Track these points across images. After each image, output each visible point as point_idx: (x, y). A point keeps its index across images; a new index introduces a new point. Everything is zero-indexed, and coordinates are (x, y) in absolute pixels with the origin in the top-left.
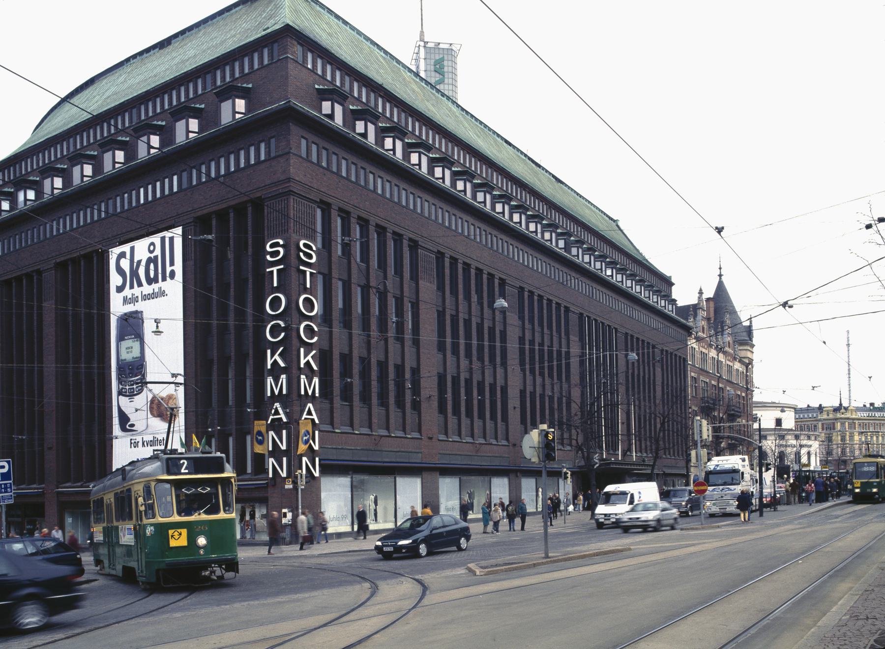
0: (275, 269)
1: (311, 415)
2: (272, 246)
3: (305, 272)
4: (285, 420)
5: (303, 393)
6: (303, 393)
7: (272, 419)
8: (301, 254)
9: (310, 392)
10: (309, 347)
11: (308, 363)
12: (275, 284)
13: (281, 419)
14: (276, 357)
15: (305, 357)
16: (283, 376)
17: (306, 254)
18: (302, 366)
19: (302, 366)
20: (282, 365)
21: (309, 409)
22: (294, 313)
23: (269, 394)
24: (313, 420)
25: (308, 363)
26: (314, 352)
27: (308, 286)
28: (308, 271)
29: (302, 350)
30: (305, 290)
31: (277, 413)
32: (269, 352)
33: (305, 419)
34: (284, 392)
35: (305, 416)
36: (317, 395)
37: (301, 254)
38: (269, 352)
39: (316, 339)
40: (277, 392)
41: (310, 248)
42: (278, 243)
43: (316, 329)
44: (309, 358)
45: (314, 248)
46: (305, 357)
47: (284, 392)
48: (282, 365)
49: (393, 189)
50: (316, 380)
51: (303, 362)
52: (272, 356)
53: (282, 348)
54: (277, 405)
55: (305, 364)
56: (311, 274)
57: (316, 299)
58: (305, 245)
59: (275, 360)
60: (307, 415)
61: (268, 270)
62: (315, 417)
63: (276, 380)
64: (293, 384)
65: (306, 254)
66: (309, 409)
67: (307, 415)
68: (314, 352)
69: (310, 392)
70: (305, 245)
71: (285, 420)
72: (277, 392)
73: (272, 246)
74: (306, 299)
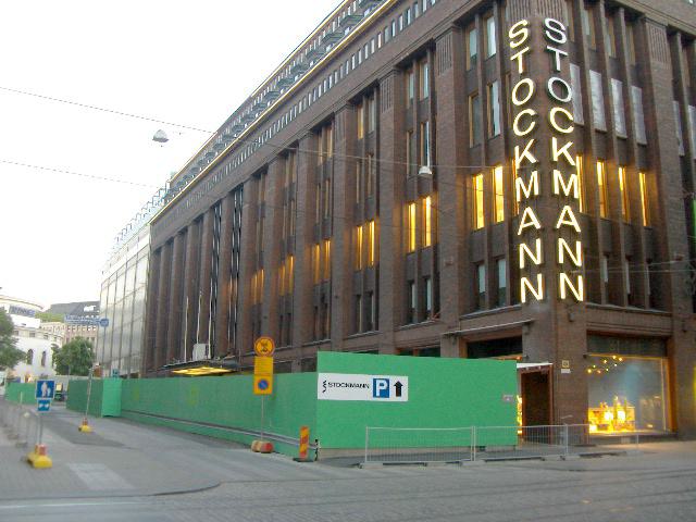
0: (519, 55)
2: (515, 31)
4: (538, 226)
8: (548, 33)
9: (567, 192)
10: (563, 138)
11: (562, 157)
12: (521, 70)
13: (533, 227)
14: (526, 153)
15: (559, 148)
16: (535, 175)
17: (552, 33)
18: (555, 159)
19: (555, 159)
20: (532, 160)
21: (567, 213)
22: (542, 98)
23: (518, 199)
24: (572, 228)
25: (562, 157)
27: (558, 68)
28: (558, 52)
29: (554, 141)
30: (556, 72)
31: (528, 219)
32: (517, 149)
33: (563, 225)
34: (536, 192)
35: (561, 221)
36: (576, 196)
37: (548, 33)
38: (517, 149)
39: (570, 130)
40: (527, 194)
41: (558, 27)
44: (564, 150)
45: (563, 28)
46: (559, 148)
47: (536, 192)
48: (532, 160)
52: (521, 151)
53: (532, 141)
54: (529, 210)
55: (559, 157)
57: (569, 83)
58: (551, 23)
61: (512, 58)
63: (526, 183)
64: (546, 181)
65: (552, 33)
66: (567, 213)
68: (569, 144)
70: (551, 23)
71: (538, 226)
72: (527, 194)
73: (515, 31)
74: (555, 83)
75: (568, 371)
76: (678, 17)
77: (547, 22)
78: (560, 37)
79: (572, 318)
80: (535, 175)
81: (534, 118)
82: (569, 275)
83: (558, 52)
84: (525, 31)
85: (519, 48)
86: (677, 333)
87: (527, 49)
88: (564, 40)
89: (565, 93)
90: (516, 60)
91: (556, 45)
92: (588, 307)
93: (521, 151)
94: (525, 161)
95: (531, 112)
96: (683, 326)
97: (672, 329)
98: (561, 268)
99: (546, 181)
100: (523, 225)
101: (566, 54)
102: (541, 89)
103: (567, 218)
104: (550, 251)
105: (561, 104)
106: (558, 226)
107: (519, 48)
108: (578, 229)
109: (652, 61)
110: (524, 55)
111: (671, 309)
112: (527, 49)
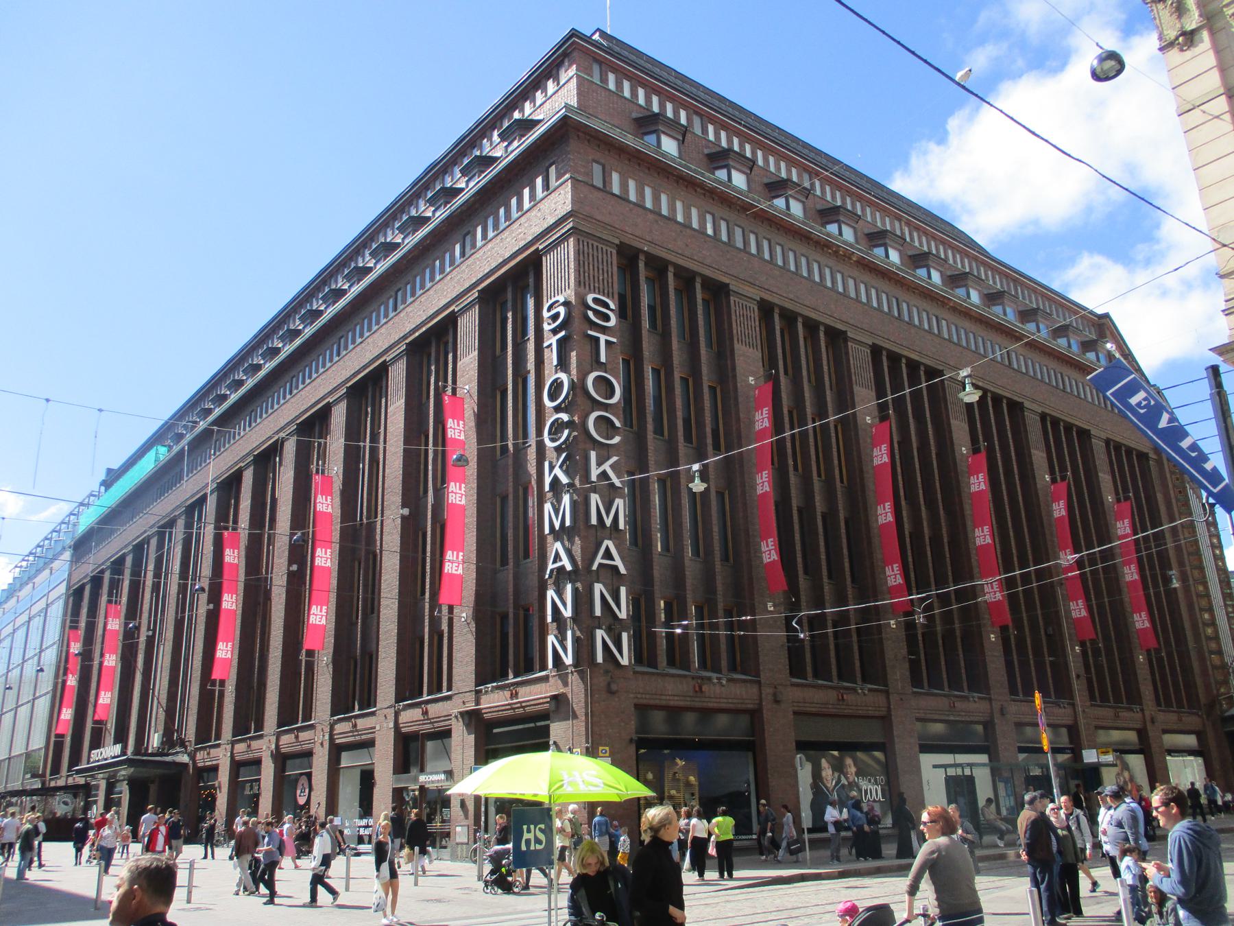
1: (612, 559)
3: (597, 339)
4: (569, 567)
5: (594, 521)
6: (594, 521)
7: (552, 571)
8: (590, 314)
9: (608, 522)
11: (604, 475)
13: (563, 567)
15: (599, 464)
16: (566, 499)
20: (564, 479)
21: (607, 549)
22: (581, 400)
24: (616, 568)
25: (604, 475)
26: (615, 459)
27: (603, 359)
28: (603, 338)
29: (593, 455)
30: (598, 365)
31: (557, 558)
33: (600, 564)
34: (568, 523)
35: (599, 560)
36: (622, 526)
37: (590, 314)
39: (617, 440)
40: (557, 525)
41: (606, 306)
42: (557, 301)
43: (618, 424)
44: (606, 467)
45: (612, 306)
46: (599, 464)
47: (568, 523)
48: (564, 479)
49: (746, 238)
50: (619, 503)
51: (594, 473)
52: (552, 468)
55: (598, 476)
56: (607, 342)
57: (617, 378)
58: (595, 300)
59: (555, 476)
60: (602, 558)
62: (618, 562)
67: (602, 558)
68: (615, 459)
69: (608, 522)
70: (595, 300)
71: (569, 567)
72: (557, 525)
73: (549, 310)
75: (678, 761)
76: (775, 290)
77: (590, 299)
78: (607, 318)
79: (614, 687)
80: (566, 499)
81: (570, 424)
82: (609, 630)
83: (603, 338)
84: (562, 310)
85: (555, 332)
86: (767, 705)
87: (563, 333)
88: (613, 322)
89: (612, 393)
90: (550, 345)
91: (604, 330)
92: (635, 673)
93: (552, 468)
94: (556, 481)
95: (565, 417)
96: (775, 695)
97: (761, 700)
98: (598, 623)
99: (581, 508)
100: (551, 566)
101: (614, 340)
102: (578, 387)
103: (608, 555)
104: (582, 601)
105: (606, 407)
106: (595, 567)
107: (555, 332)
108: (623, 570)
109: (737, 346)
110: (559, 341)
111: (758, 675)
112: (563, 333)
